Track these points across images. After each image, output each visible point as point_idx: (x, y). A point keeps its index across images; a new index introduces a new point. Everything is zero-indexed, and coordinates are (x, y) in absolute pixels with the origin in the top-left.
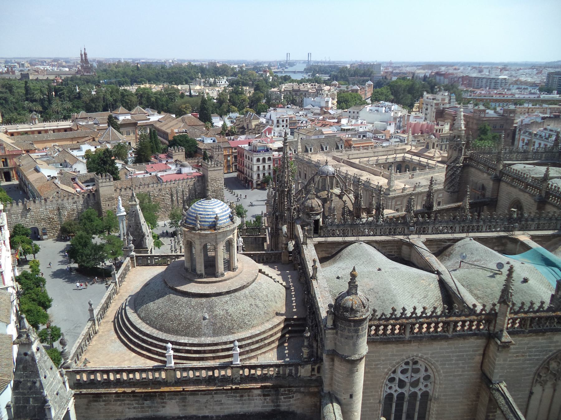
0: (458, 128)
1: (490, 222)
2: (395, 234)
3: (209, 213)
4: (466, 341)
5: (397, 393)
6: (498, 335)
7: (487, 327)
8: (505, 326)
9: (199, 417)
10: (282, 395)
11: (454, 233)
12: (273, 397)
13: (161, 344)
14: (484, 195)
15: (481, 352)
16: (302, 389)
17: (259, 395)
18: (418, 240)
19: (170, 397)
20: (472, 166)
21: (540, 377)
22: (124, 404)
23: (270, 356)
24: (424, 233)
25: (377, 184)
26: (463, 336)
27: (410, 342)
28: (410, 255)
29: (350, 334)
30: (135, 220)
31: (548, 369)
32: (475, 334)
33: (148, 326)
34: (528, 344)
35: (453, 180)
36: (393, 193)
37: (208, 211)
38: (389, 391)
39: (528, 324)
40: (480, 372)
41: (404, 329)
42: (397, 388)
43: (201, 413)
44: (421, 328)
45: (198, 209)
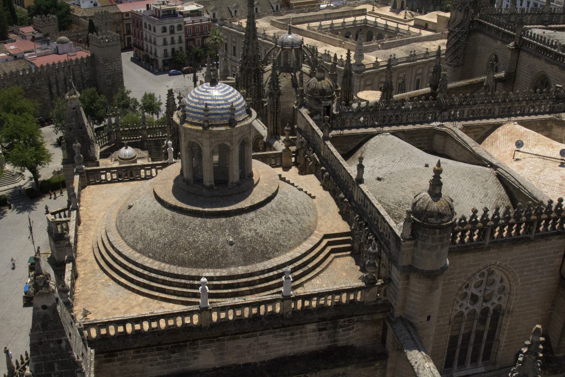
3: (220, 102)
5: (468, 311)
9: (240, 365)
10: (341, 327)
12: (330, 331)
13: (178, 280)
16: (365, 318)
17: (314, 331)
18: (455, 128)
20: (481, 32)
22: (145, 360)
23: (318, 282)
26: (546, 236)
27: (489, 248)
28: (444, 147)
29: (434, 244)
32: (558, 233)
33: (151, 260)
35: (457, 50)
37: (218, 100)
38: (459, 309)
42: (469, 305)
43: (242, 361)
45: (203, 97)
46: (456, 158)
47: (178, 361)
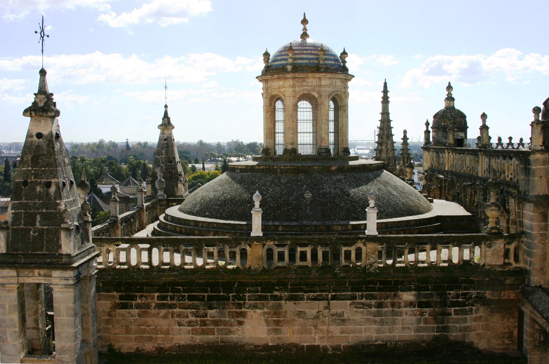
10: (454, 304)
17: (411, 304)
19: (252, 302)
30: (167, 153)
47: (216, 323)
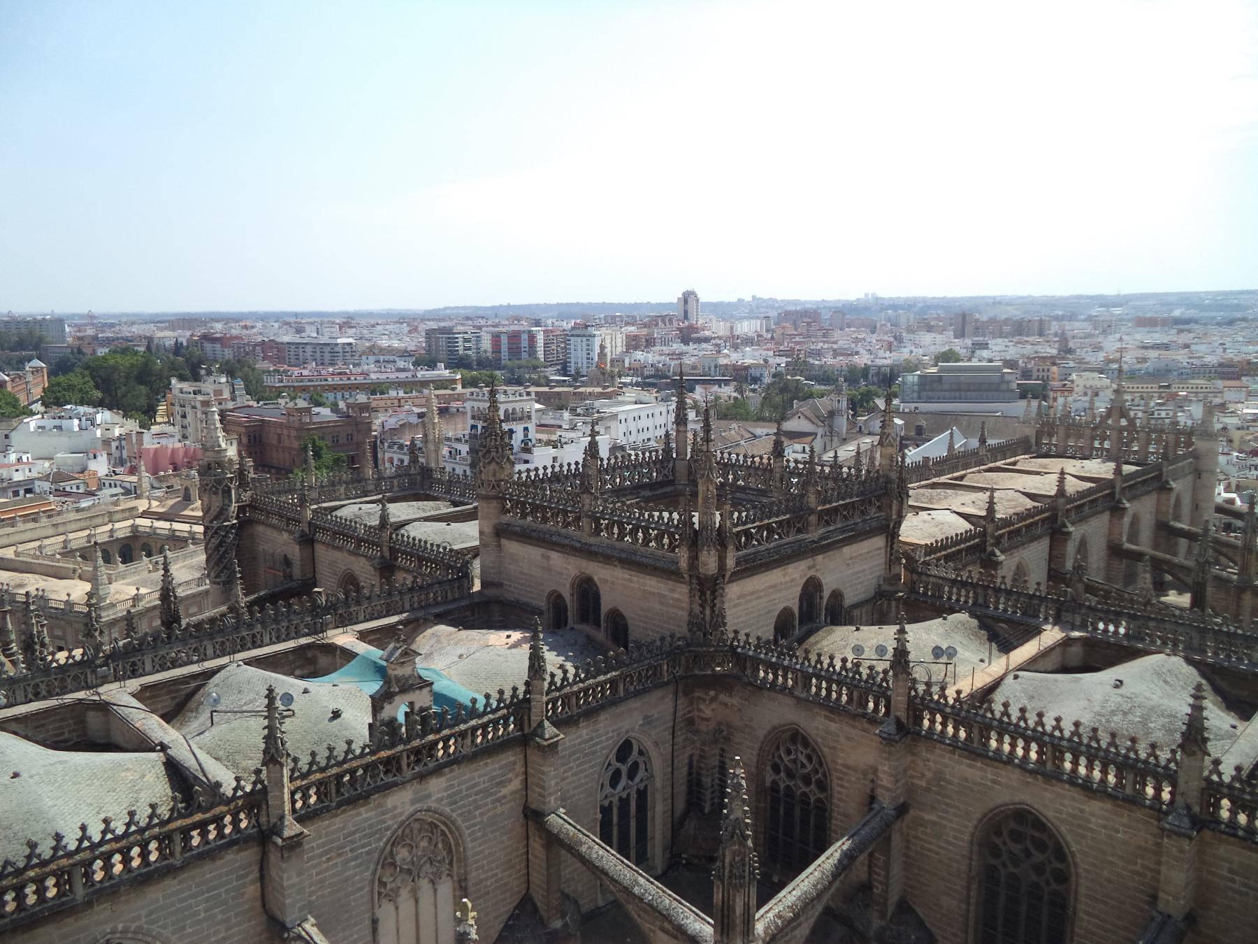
0: (213, 447)
1: (276, 621)
2: (64, 690)
4: (219, 863)
6: (277, 830)
7: (253, 821)
8: (288, 807)
11: (203, 660)
14: (289, 577)
15: (256, 874)
18: (120, 694)
20: (260, 522)
21: (385, 884)
24: (134, 674)
25: (66, 598)
26: (209, 854)
28: (109, 730)
31: (394, 865)
34: (343, 828)
35: (222, 557)
36: (111, 612)
39: (333, 791)
40: (264, 918)
41: (69, 881)
44: (108, 867)
46: (125, 745)
